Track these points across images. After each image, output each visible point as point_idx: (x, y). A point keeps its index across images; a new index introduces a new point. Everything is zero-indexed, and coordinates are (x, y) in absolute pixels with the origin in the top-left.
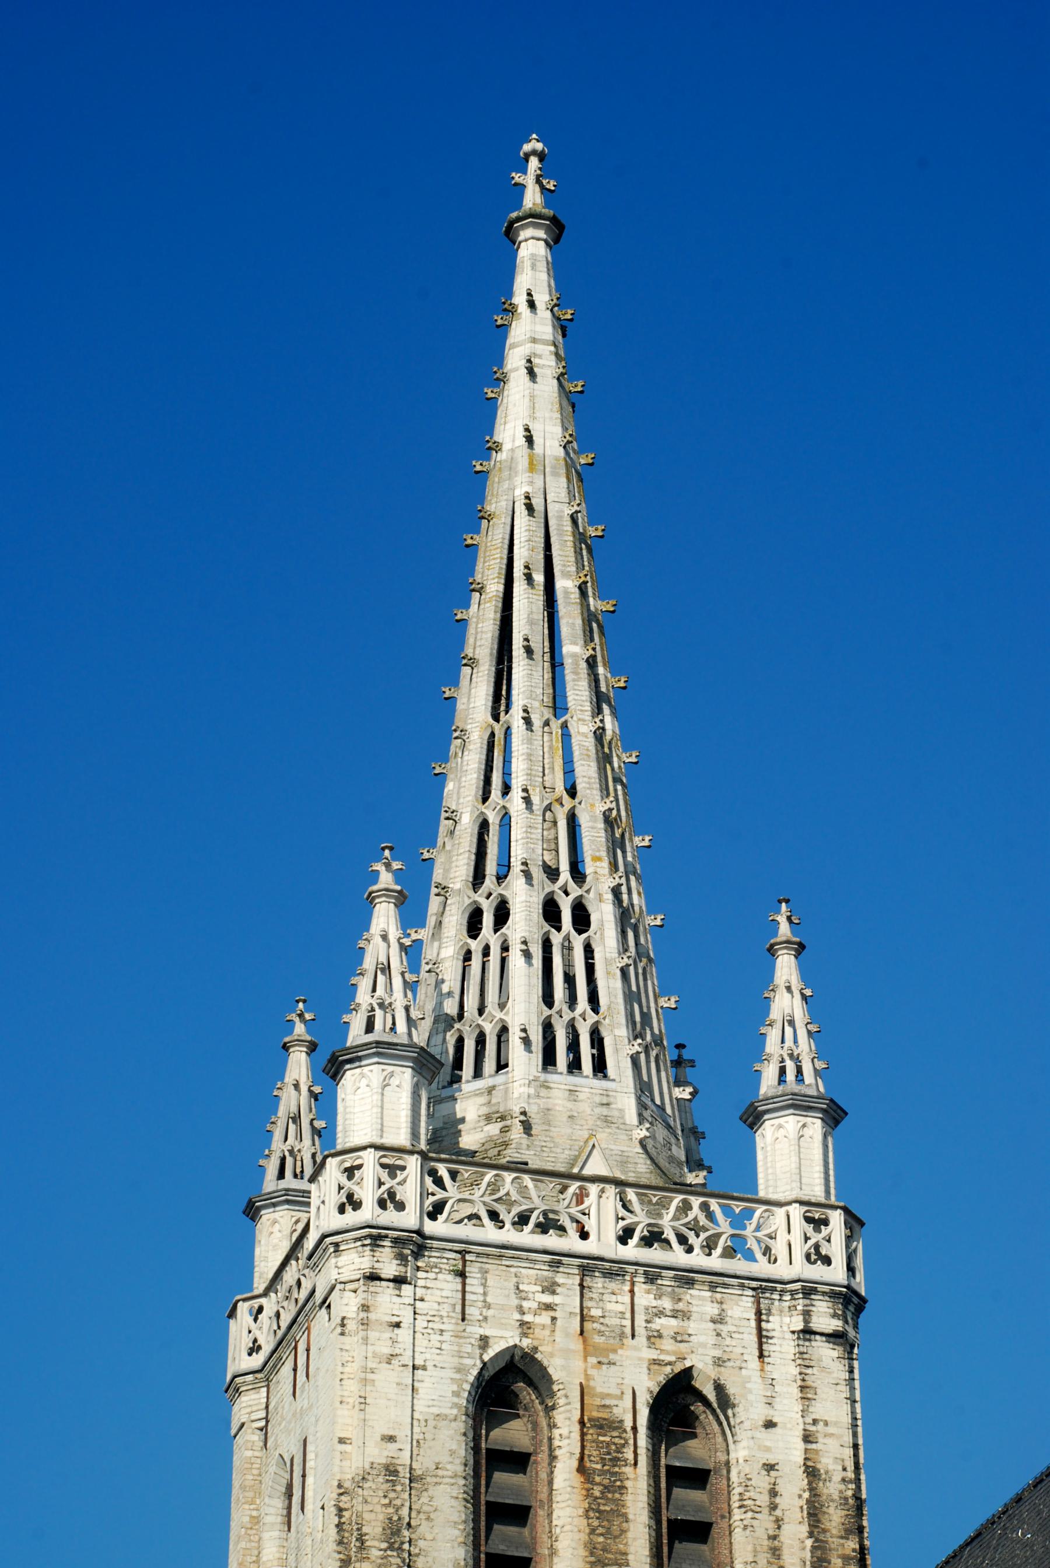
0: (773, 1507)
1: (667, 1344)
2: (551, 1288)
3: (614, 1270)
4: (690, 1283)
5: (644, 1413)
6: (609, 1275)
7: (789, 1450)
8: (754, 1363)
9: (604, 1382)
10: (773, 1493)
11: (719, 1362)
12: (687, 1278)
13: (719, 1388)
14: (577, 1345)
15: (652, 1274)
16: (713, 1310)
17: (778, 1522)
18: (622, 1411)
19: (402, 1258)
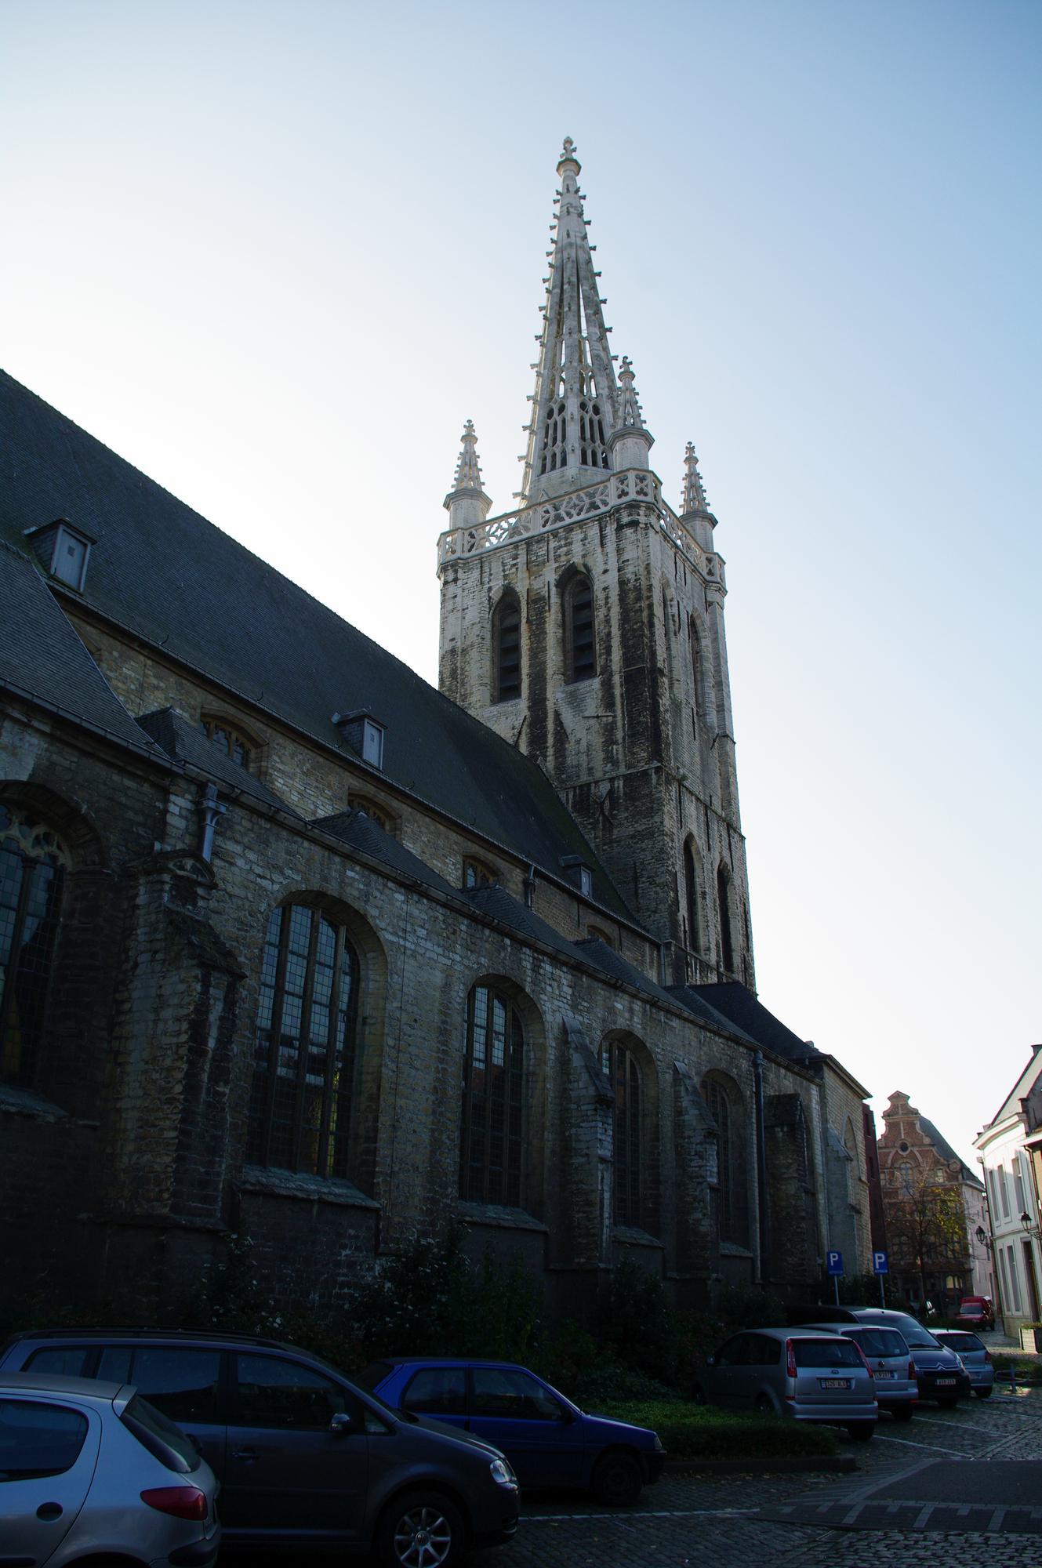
0: (607, 603)
1: (563, 558)
2: (515, 557)
3: (540, 539)
4: (572, 530)
5: (553, 589)
6: (538, 542)
7: (612, 579)
8: (599, 550)
9: (537, 584)
10: (607, 598)
11: (584, 556)
12: (569, 529)
13: (585, 566)
14: (526, 574)
15: (555, 534)
16: (581, 536)
17: (609, 610)
18: (544, 592)
19: (456, 571)
